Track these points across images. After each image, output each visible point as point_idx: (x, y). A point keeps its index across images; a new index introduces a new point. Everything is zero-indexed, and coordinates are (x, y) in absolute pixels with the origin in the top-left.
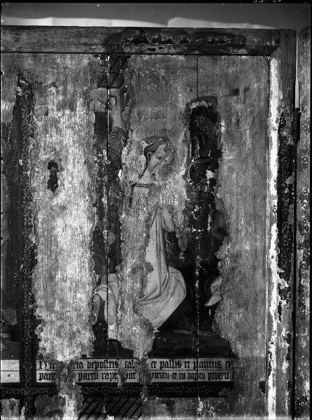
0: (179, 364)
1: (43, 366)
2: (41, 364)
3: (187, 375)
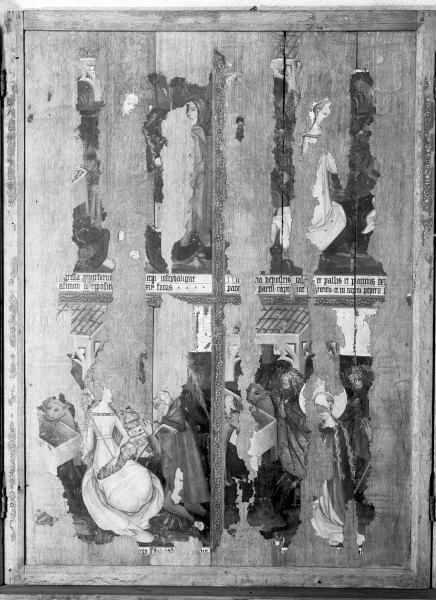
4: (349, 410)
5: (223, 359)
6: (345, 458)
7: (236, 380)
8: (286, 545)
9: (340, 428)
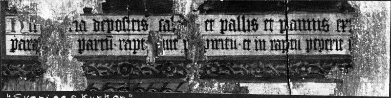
0: (254, 25)
1: (18, 27)
2: (13, 24)
3: (268, 44)
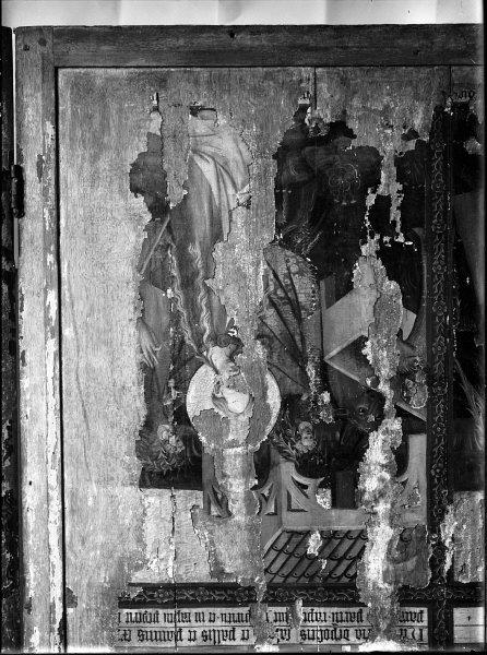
0: (205, 637)
1: (417, 632)
3: (193, 619)
4: (183, 386)
5: (430, 478)
6: (188, 283)
7: (405, 439)
8: (303, 109)
9: (200, 345)
